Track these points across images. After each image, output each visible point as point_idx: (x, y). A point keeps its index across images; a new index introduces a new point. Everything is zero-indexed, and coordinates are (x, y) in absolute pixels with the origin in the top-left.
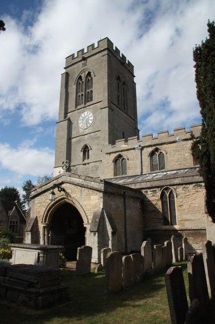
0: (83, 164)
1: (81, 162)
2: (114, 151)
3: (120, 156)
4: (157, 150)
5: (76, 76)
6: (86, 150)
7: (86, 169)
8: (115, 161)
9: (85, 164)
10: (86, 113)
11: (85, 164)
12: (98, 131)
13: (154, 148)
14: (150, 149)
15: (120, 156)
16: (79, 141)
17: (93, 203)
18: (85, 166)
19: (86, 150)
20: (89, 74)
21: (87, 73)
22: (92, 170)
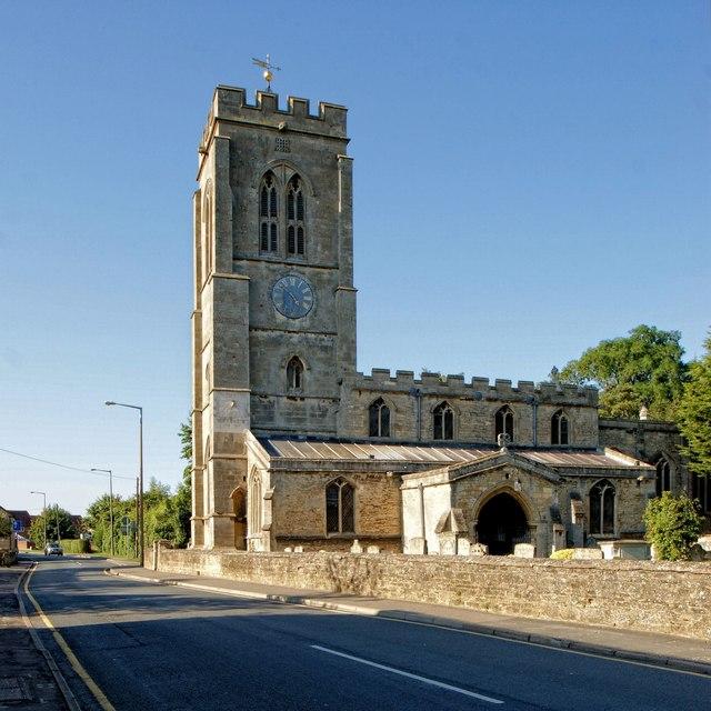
0: (288, 398)
1: (281, 389)
2: (370, 386)
3: (380, 401)
4: (444, 405)
5: (261, 167)
6: (294, 366)
7: (297, 409)
8: (374, 407)
9: (294, 398)
10: (293, 281)
11: (294, 398)
12: (326, 334)
13: (441, 401)
14: (435, 402)
15: (380, 401)
16: (276, 342)
17: (547, 496)
18: (293, 402)
19: (294, 366)
20: (296, 178)
21: (290, 173)
22: (313, 415)
